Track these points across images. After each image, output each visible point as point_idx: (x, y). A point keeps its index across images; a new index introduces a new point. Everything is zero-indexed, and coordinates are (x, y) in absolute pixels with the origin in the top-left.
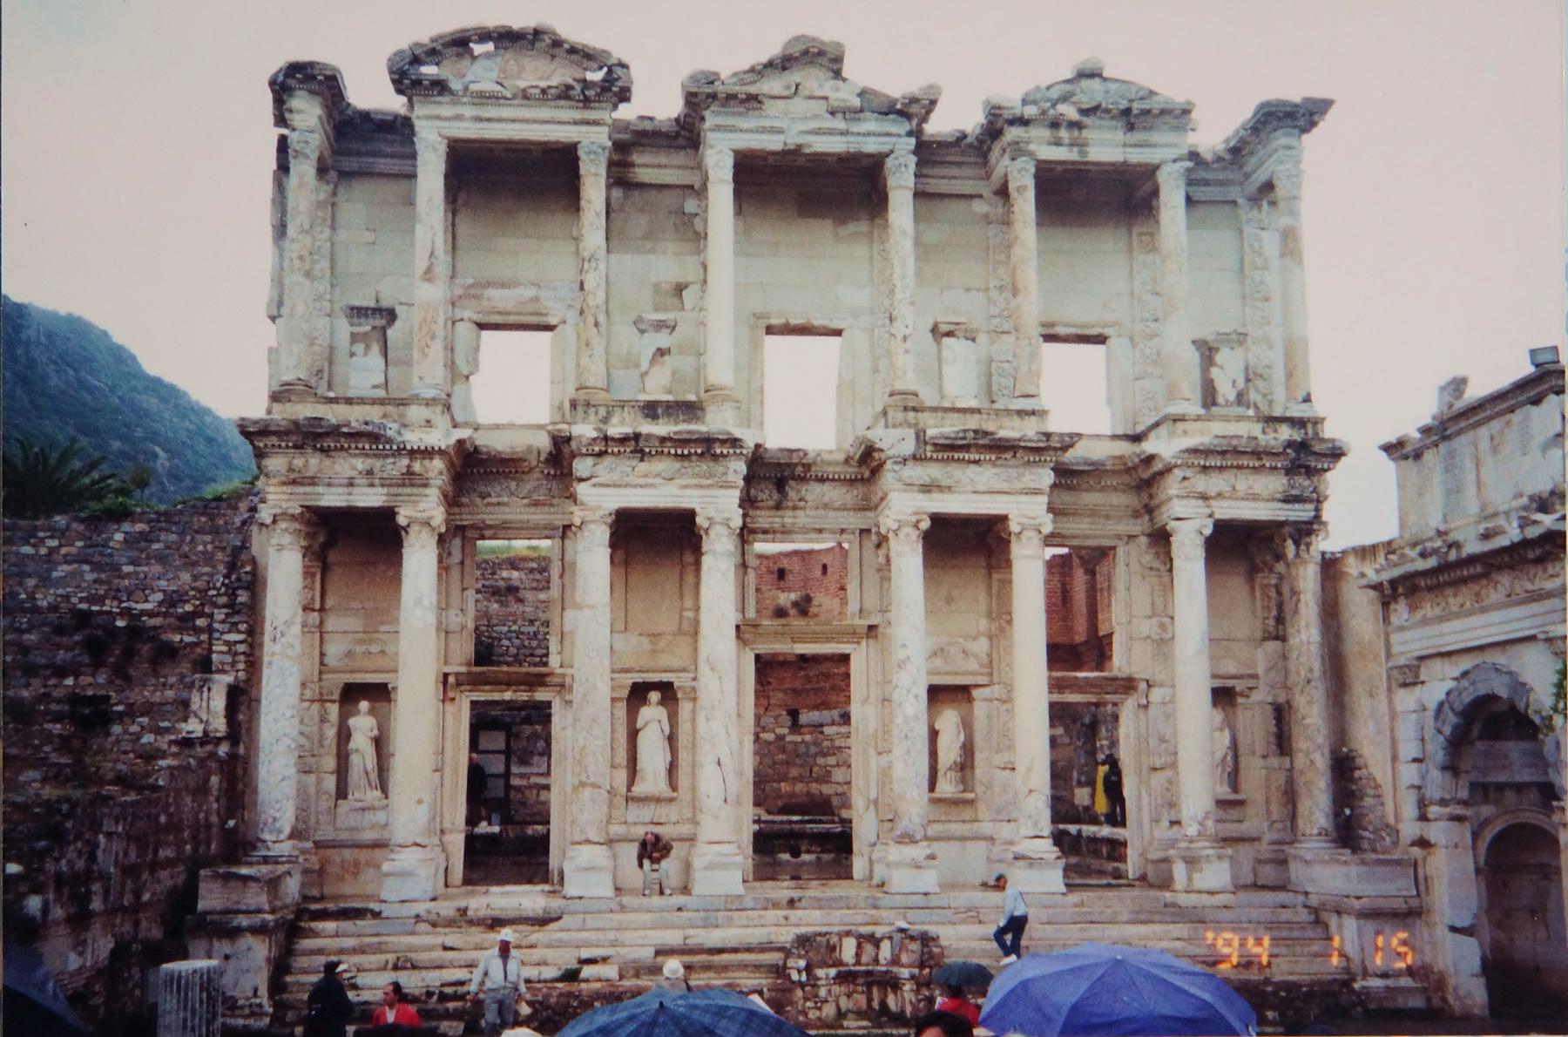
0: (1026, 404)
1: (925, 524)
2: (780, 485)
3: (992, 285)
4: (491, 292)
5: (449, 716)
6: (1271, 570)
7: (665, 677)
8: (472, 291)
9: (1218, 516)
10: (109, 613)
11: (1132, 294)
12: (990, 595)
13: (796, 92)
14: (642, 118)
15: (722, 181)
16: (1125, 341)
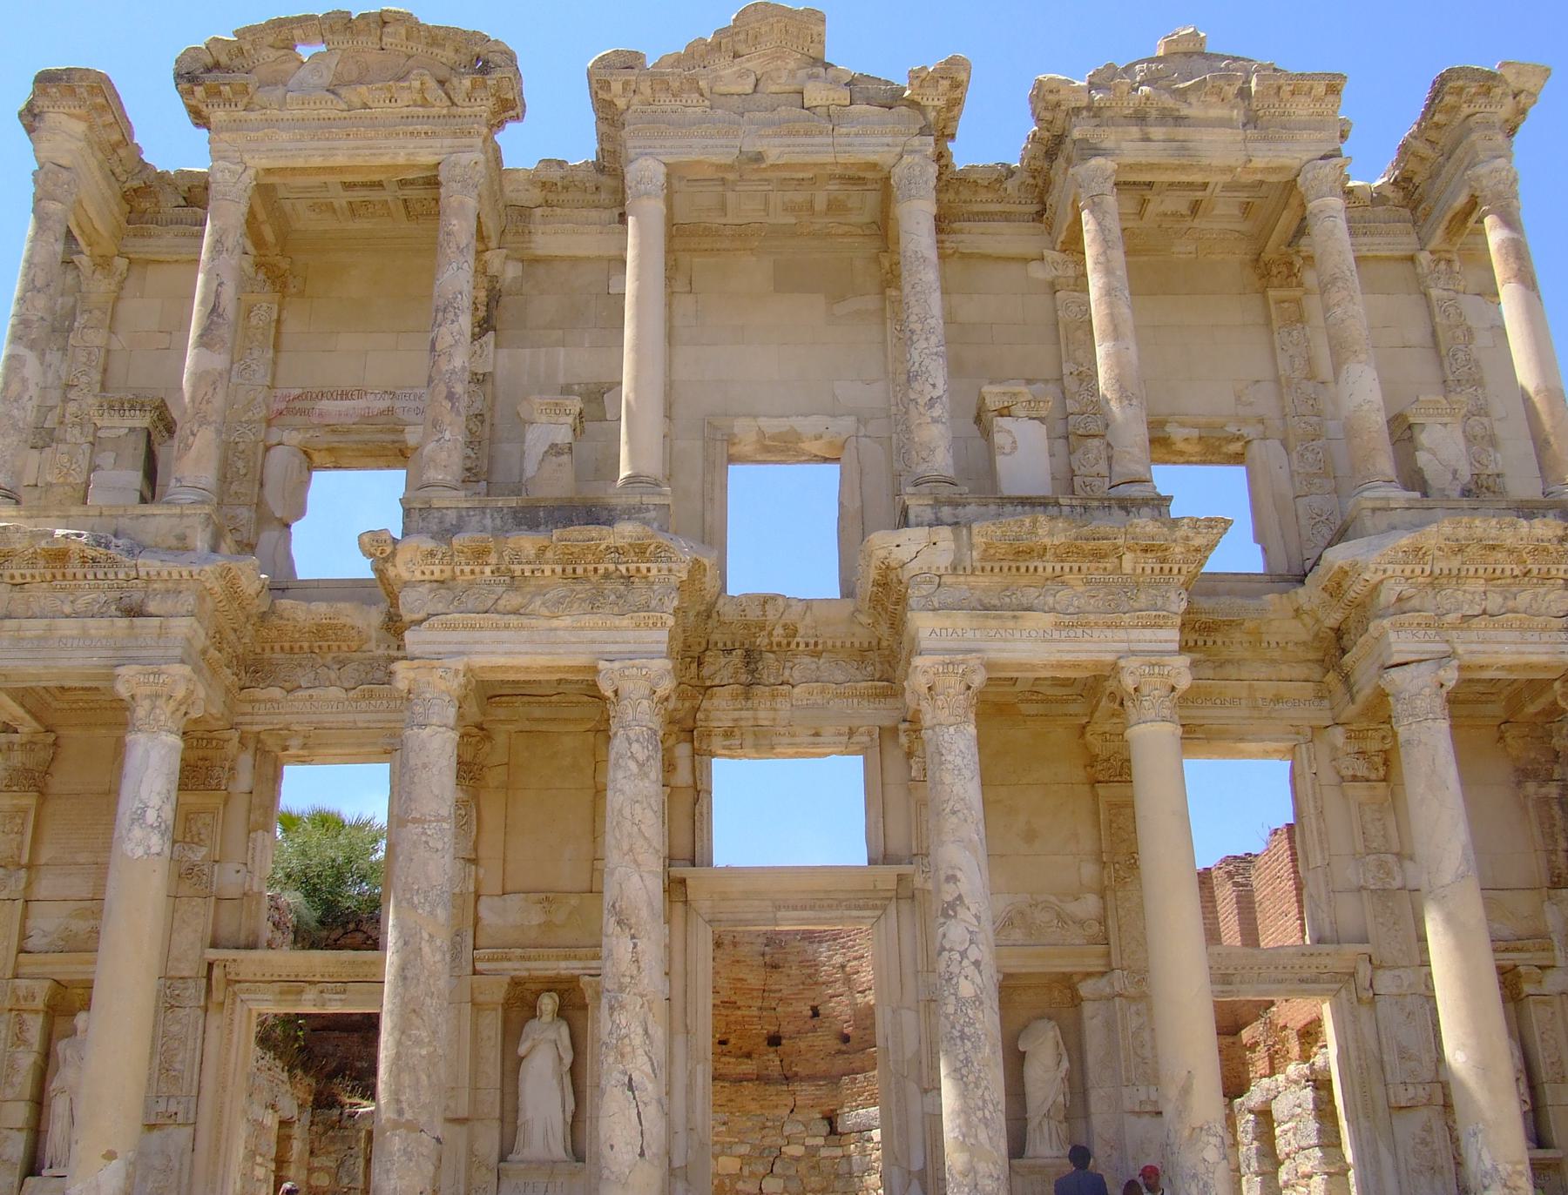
0: (1135, 491)
1: (978, 680)
2: (751, 657)
3: (1065, 371)
4: (325, 405)
5: (213, 1033)
6: (1549, 779)
7: (565, 968)
8: (298, 405)
9: (1467, 659)
11: (1277, 380)
12: (1097, 824)
13: (755, 91)
14: (547, 162)
15: (648, 194)
16: (1275, 445)
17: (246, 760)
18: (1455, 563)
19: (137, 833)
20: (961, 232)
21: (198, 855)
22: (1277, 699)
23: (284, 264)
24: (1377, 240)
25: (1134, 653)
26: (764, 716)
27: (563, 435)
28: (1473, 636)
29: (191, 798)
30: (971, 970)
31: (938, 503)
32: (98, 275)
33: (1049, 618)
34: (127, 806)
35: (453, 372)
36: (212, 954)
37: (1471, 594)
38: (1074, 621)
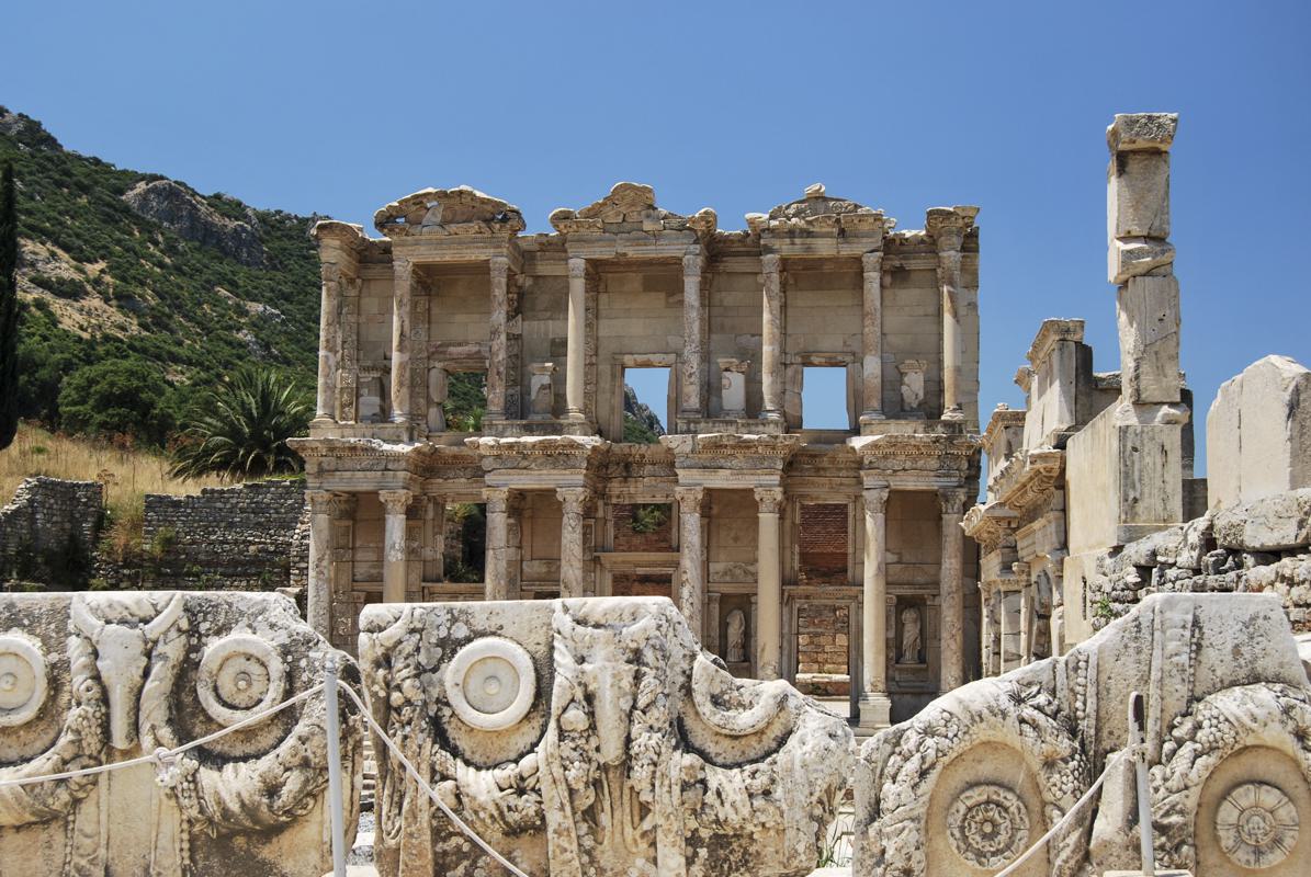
1: (700, 496)
2: (627, 466)
4: (452, 349)
8: (441, 349)
10: (265, 543)
13: (624, 220)
14: (541, 235)
17: (431, 506)
18: (892, 450)
19: (393, 553)
20: (726, 262)
21: (415, 545)
22: (841, 484)
23: (429, 281)
24: (919, 261)
25: (761, 486)
26: (632, 490)
27: (546, 380)
28: (898, 478)
29: (411, 522)
30: (689, 606)
31: (689, 423)
32: (350, 288)
33: (729, 471)
34: (388, 543)
35: (499, 362)
36: (424, 584)
37: (895, 464)
38: (740, 471)
